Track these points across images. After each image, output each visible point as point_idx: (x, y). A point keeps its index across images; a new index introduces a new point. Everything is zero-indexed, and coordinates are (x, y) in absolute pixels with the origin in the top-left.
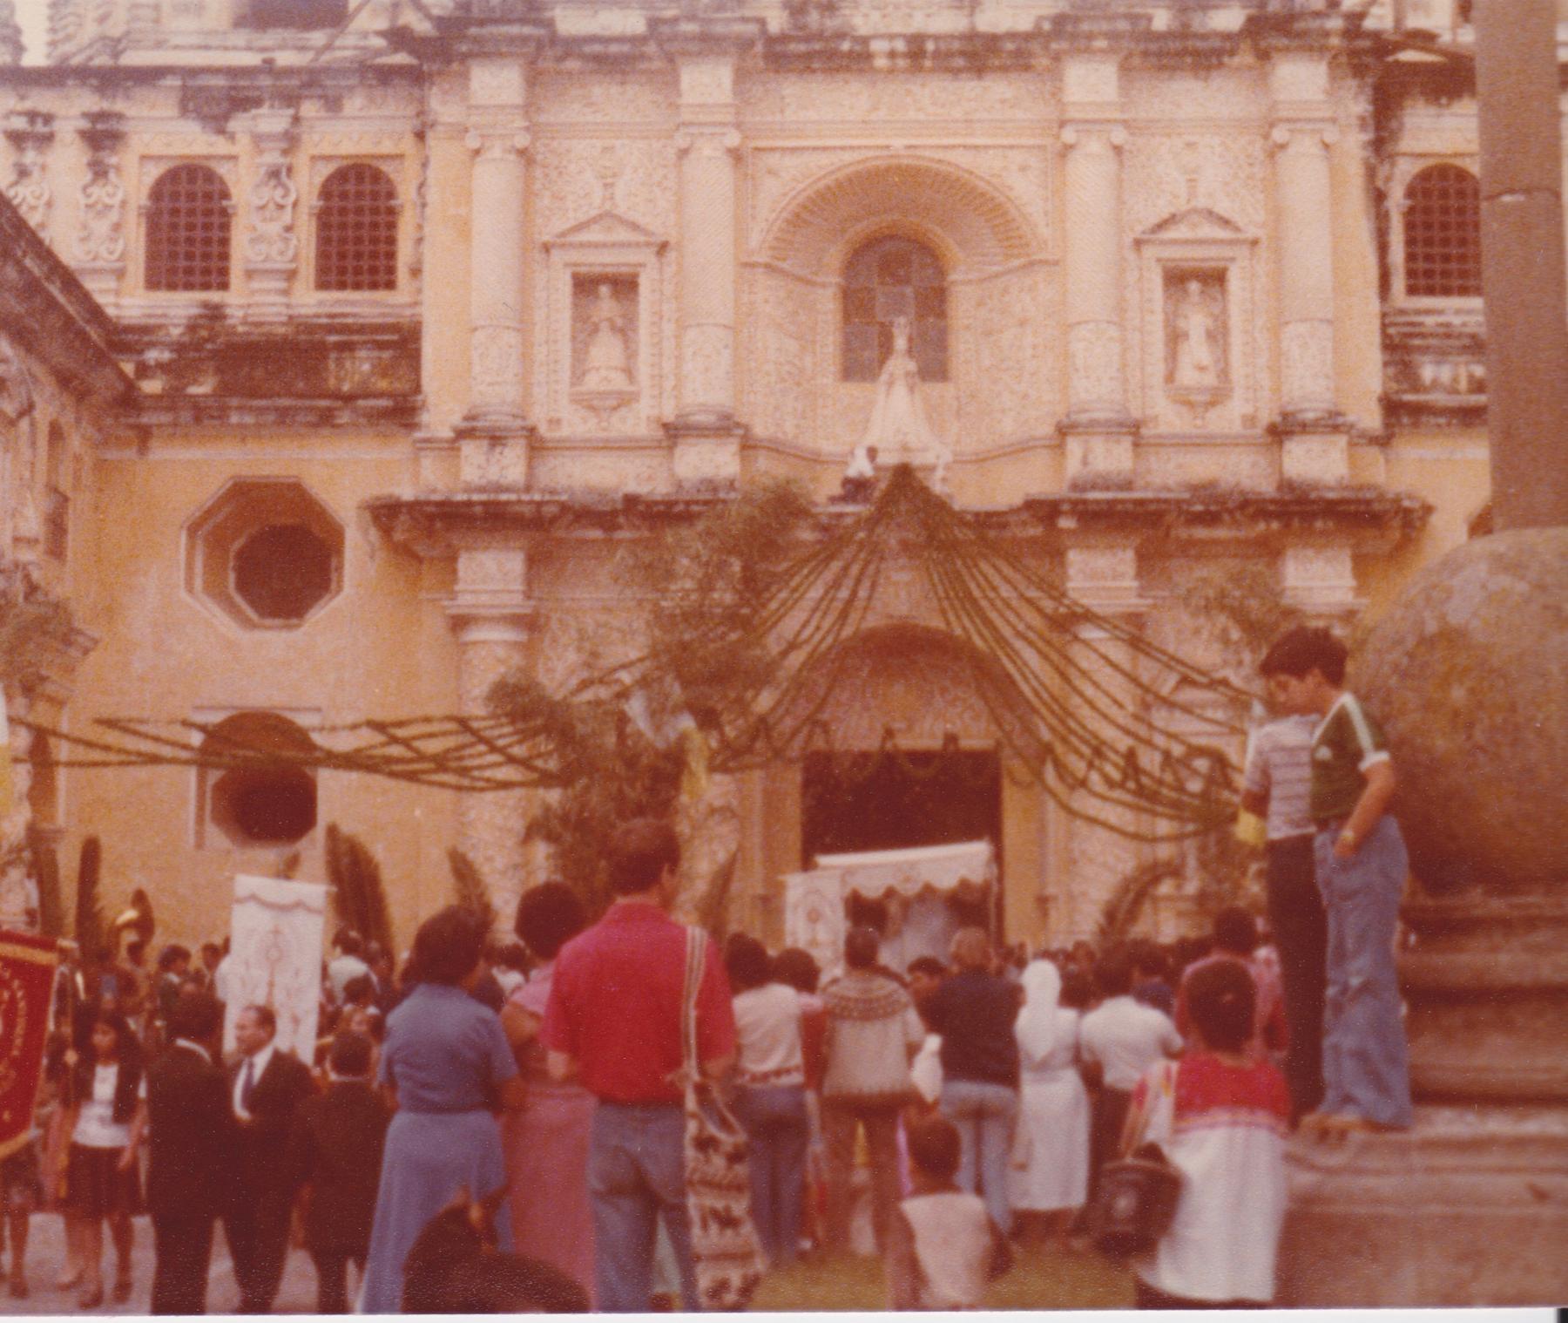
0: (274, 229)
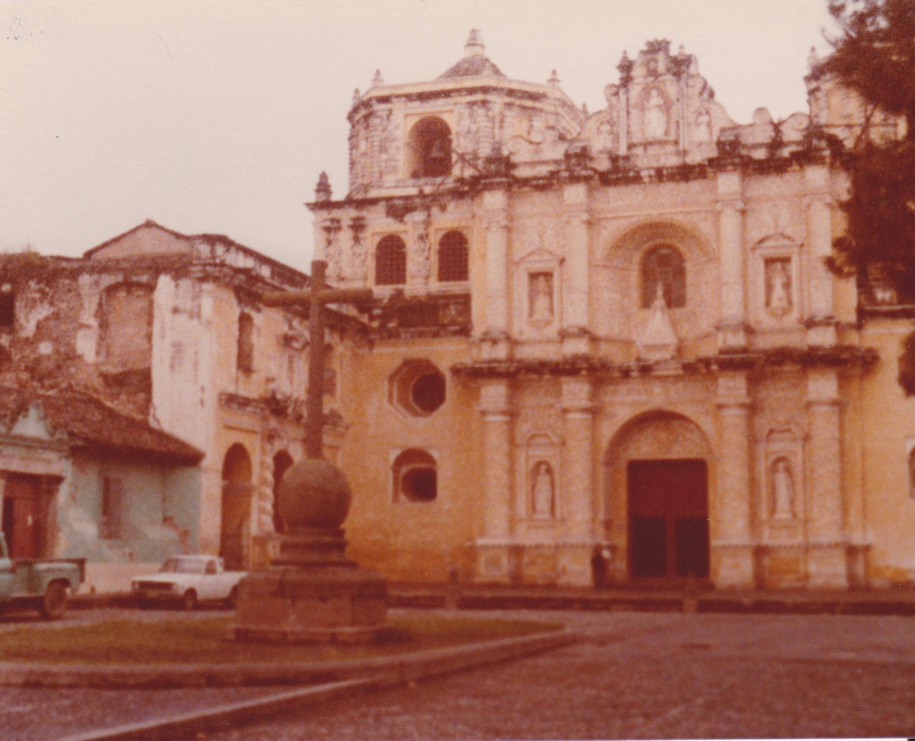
0: (421, 259)
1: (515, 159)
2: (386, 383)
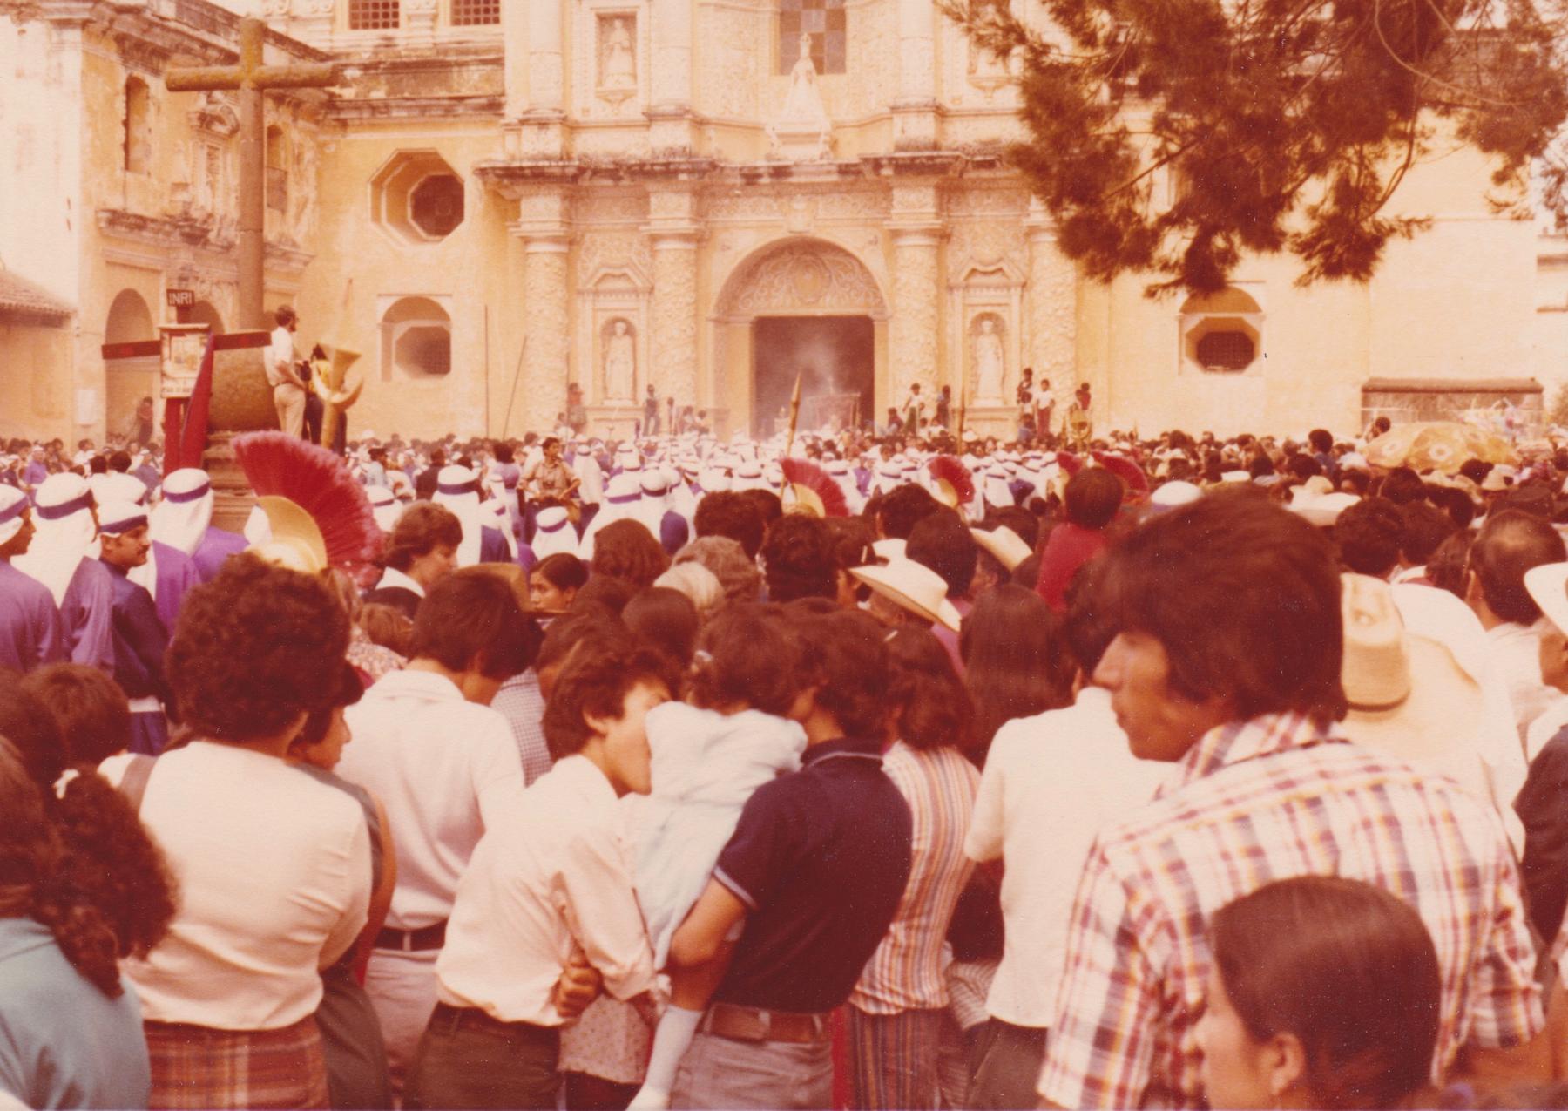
2: (369, 189)
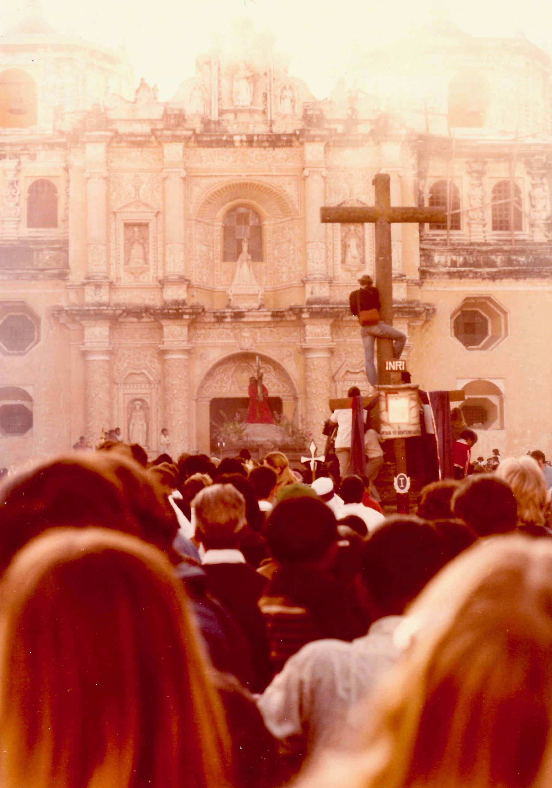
0: (12, 205)
1: (113, 115)
